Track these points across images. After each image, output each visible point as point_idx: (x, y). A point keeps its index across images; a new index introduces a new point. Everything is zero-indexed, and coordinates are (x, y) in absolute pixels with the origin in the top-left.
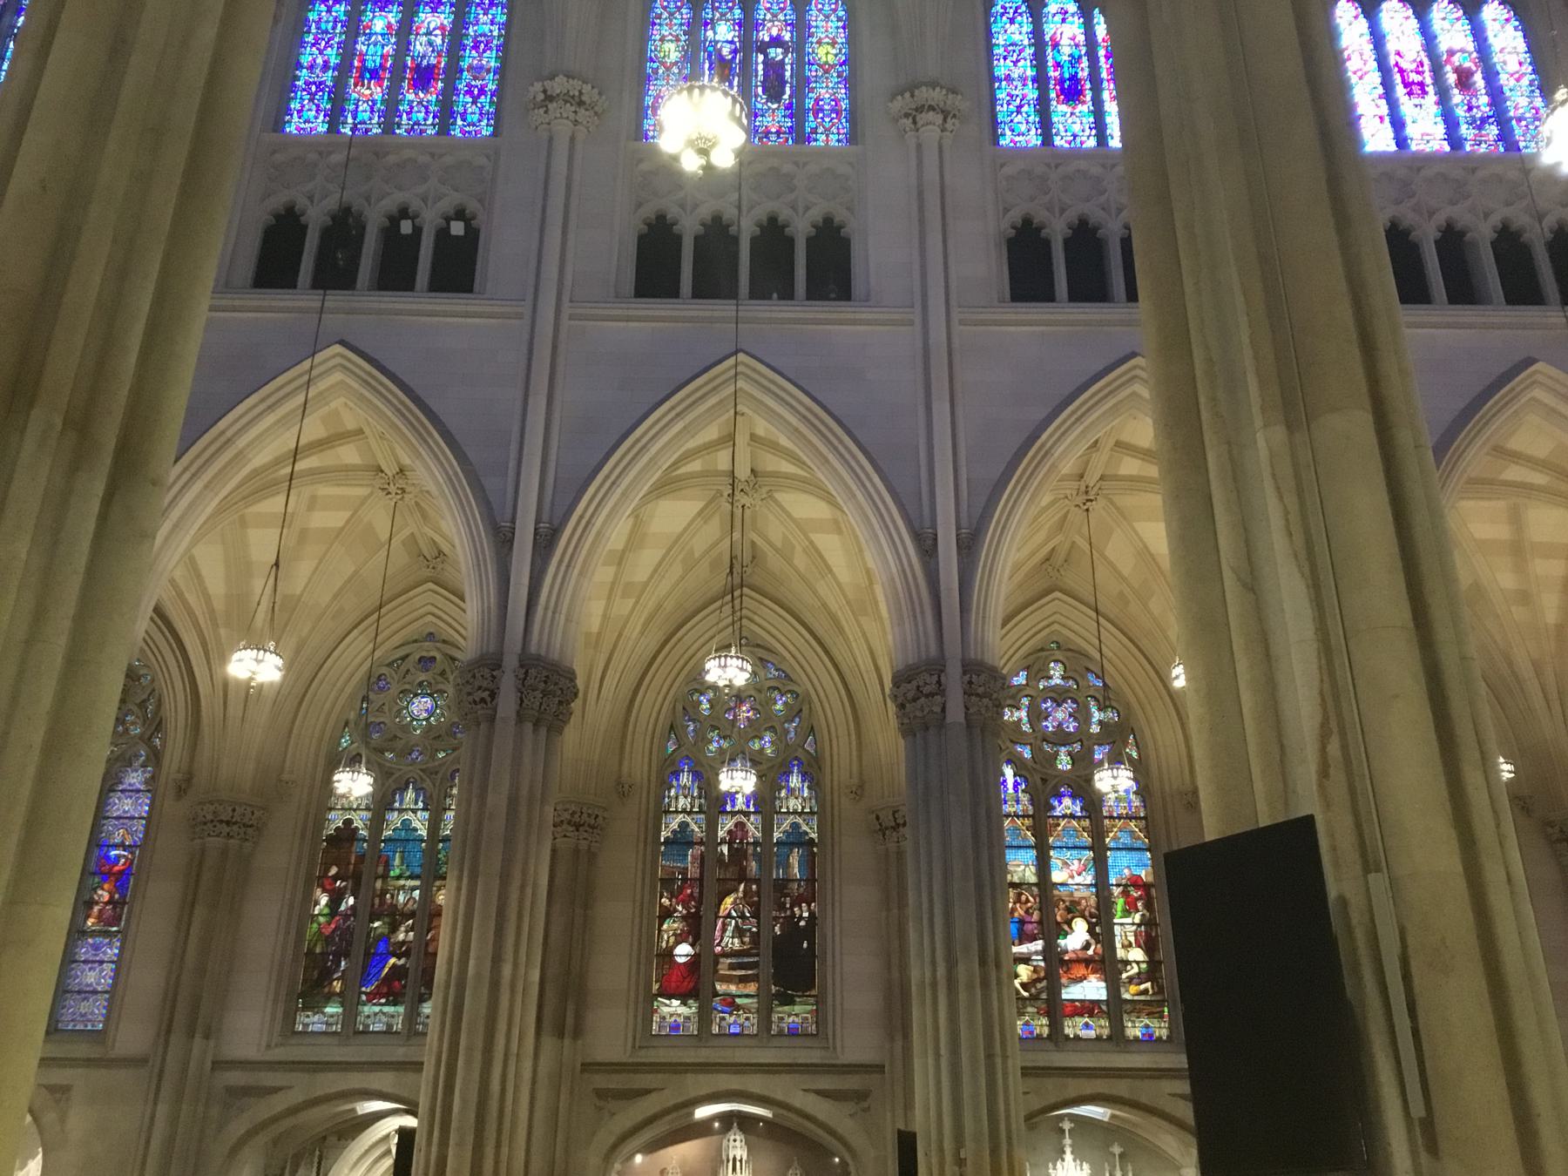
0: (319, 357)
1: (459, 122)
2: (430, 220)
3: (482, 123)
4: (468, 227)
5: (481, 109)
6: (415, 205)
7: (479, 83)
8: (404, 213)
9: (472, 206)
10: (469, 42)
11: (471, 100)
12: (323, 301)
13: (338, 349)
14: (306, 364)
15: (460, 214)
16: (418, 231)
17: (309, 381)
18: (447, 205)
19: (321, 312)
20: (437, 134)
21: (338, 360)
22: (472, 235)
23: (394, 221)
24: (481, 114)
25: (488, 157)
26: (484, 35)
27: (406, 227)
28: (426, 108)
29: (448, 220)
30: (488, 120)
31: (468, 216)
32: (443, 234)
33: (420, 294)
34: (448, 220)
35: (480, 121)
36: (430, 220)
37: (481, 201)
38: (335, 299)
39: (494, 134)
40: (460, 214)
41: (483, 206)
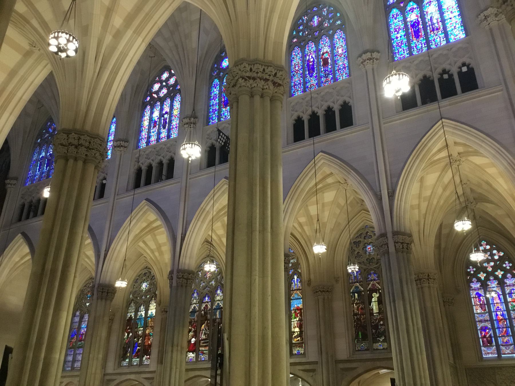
2: (454, 71)
6: (448, 67)
8: (444, 72)
9: (468, 61)
15: (464, 65)
16: (451, 76)
18: (459, 64)
23: (441, 75)
32: (460, 73)
34: (460, 68)
36: (454, 71)
40: (464, 65)
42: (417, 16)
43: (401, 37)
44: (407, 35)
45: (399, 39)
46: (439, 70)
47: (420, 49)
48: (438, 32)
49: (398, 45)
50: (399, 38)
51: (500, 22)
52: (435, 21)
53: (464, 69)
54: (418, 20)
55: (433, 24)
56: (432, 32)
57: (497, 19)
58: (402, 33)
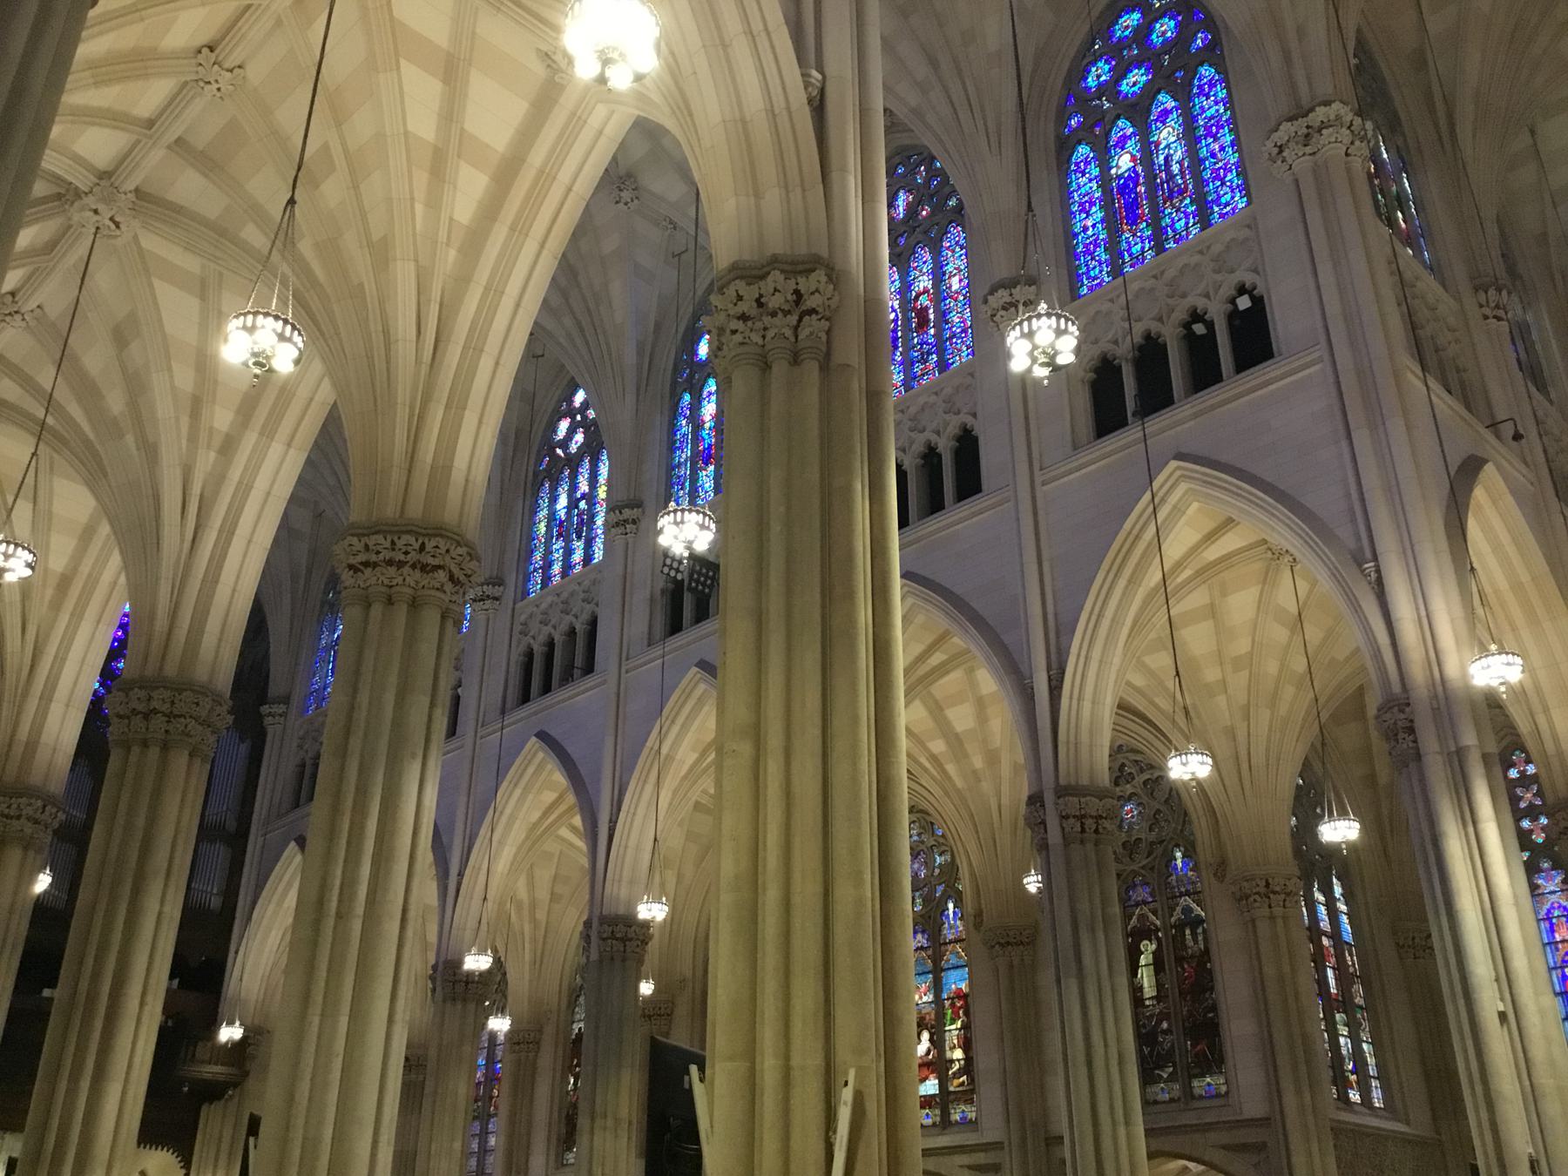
0: (1156, 484)
1: (1216, 209)
2: (1217, 311)
3: (1236, 199)
4: (1252, 298)
5: (1230, 187)
6: (1201, 303)
7: (1220, 164)
8: (1196, 316)
9: (1249, 279)
10: (1202, 132)
11: (1219, 183)
12: (1144, 429)
13: (1173, 464)
14: (1148, 496)
15: (1242, 290)
16: (1210, 325)
17: (1155, 509)
18: (1227, 290)
19: (1145, 440)
20: (1202, 229)
21: (1178, 473)
22: (1258, 302)
23: (1187, 326)
24: (1232, 191)
25: (1249, 226)
26: (1212, 117)
27: (1199, 329)
28: (1184, 212)
29: (1233, 301)
30: (1240, 192)
31: (1250, 289)
32: (1234, 315)
33: (1231, 380)
35: (1233, 198)
36: (1217, 311)
37: (1256, 271)
38: (1156, 423)
39: (1249, 203)
40: (1242, 290)
41: (1258, 273)
42: (1133, 159)
43: (1094, 226)
44: (1110, 222)
45: (1090, 232)
46: (1180, 315)
47: (1137, 257)
48: (1181, 201)
49: (1087, 252)
50: (1091, 229)
51: (1318, 156)
52: (1175, 168)
53: (1244, 303)
54: (1135, 171)
55: (1171, 176)
56: (1168, 203)
57: (1308, 150)
58: (1097, 214)
